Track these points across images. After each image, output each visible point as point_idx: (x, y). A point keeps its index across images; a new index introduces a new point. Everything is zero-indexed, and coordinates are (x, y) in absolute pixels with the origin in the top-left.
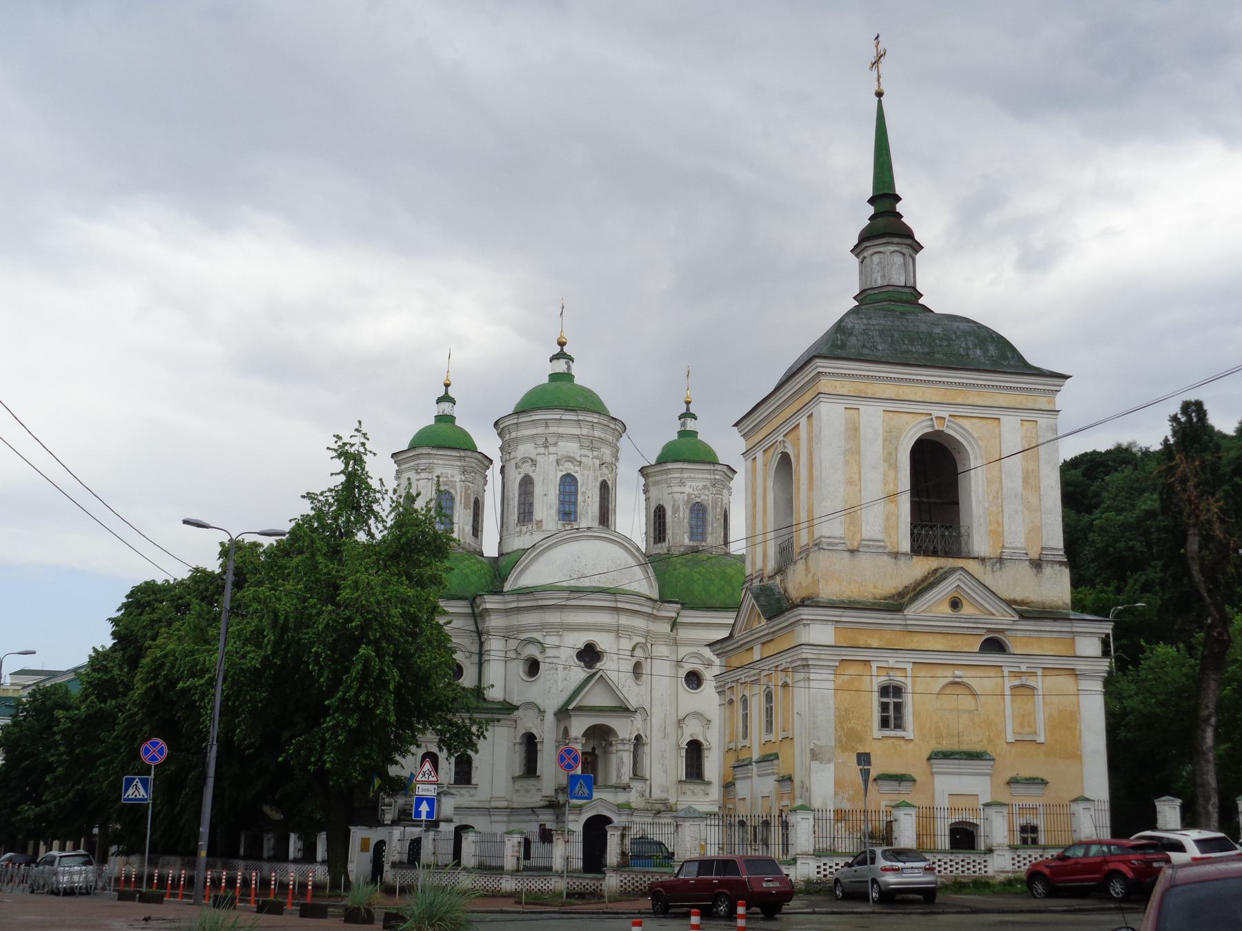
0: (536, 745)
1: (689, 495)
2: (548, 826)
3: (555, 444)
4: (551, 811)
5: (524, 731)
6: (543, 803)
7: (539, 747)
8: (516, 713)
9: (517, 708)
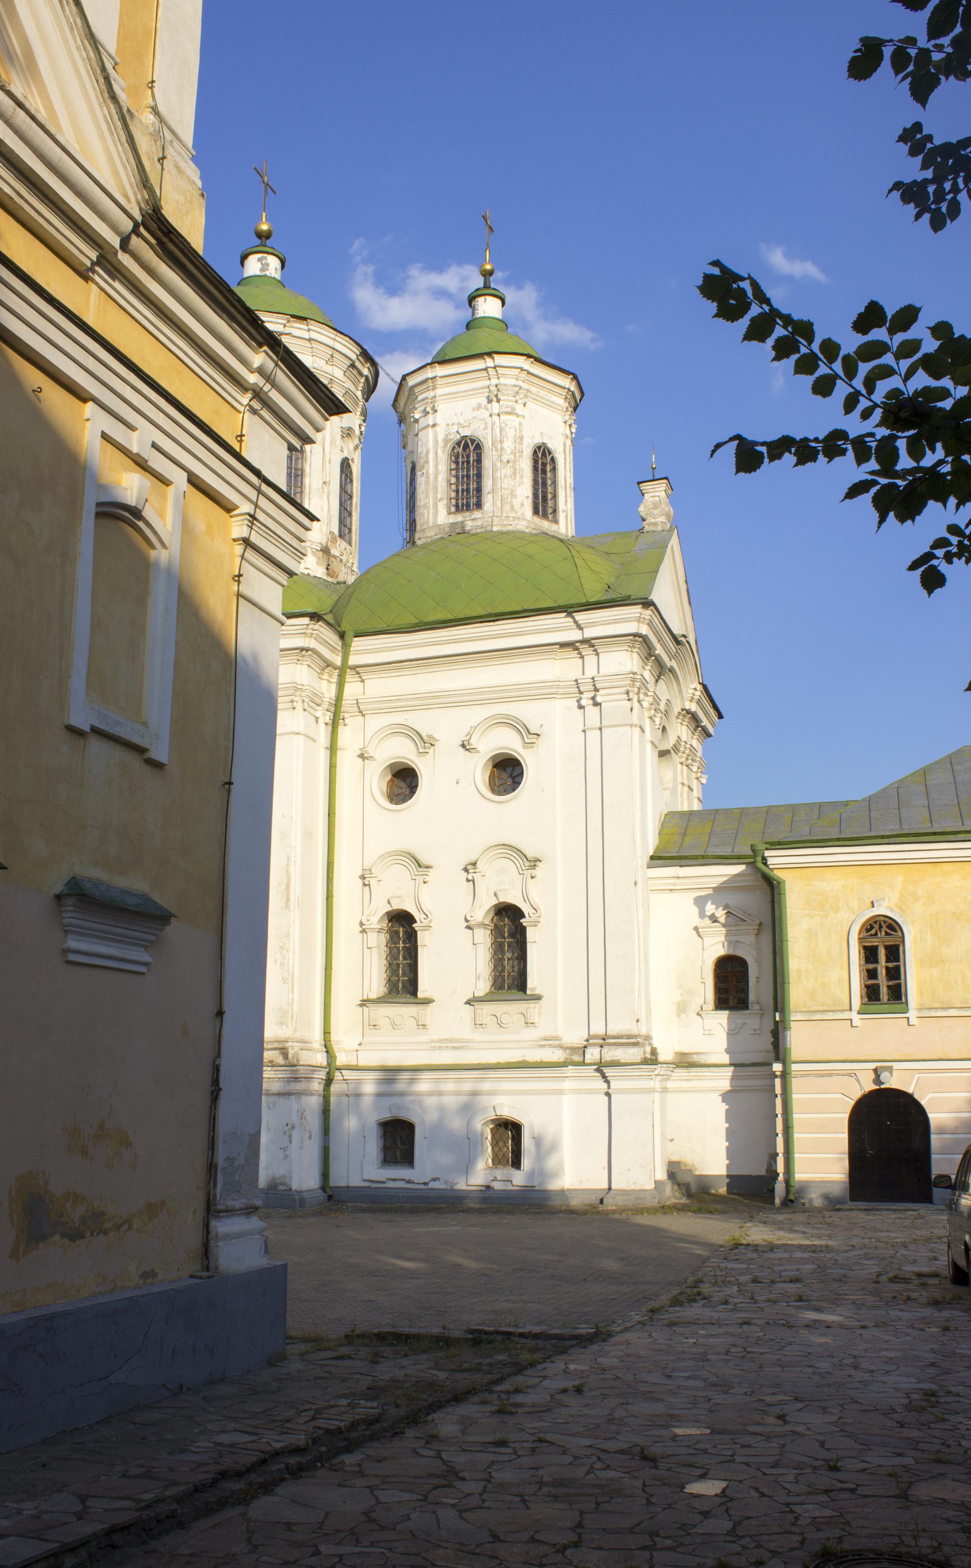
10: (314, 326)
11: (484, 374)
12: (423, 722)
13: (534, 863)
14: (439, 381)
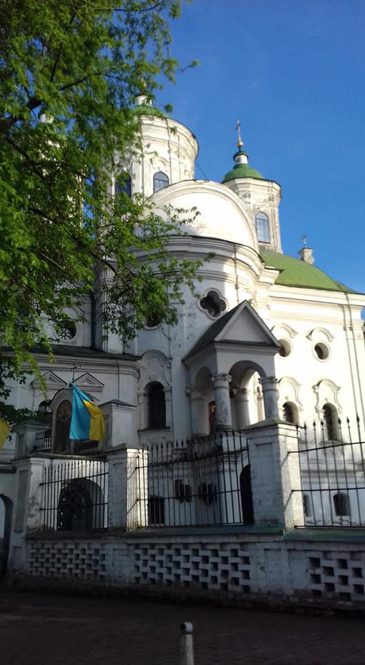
0: (164, 394)
1: (254, 205)
2: (186, 482)
3: (148, 146)
4: (186, 465)
5: (148, 381)
6: (175, 457)
7: (167, 396)
8: (139, 362)
9: (140, 358)
10: (195, 142)
11: (267, 188)
12: (293, 324)
13: (339, 388)
14: (251, 186)
